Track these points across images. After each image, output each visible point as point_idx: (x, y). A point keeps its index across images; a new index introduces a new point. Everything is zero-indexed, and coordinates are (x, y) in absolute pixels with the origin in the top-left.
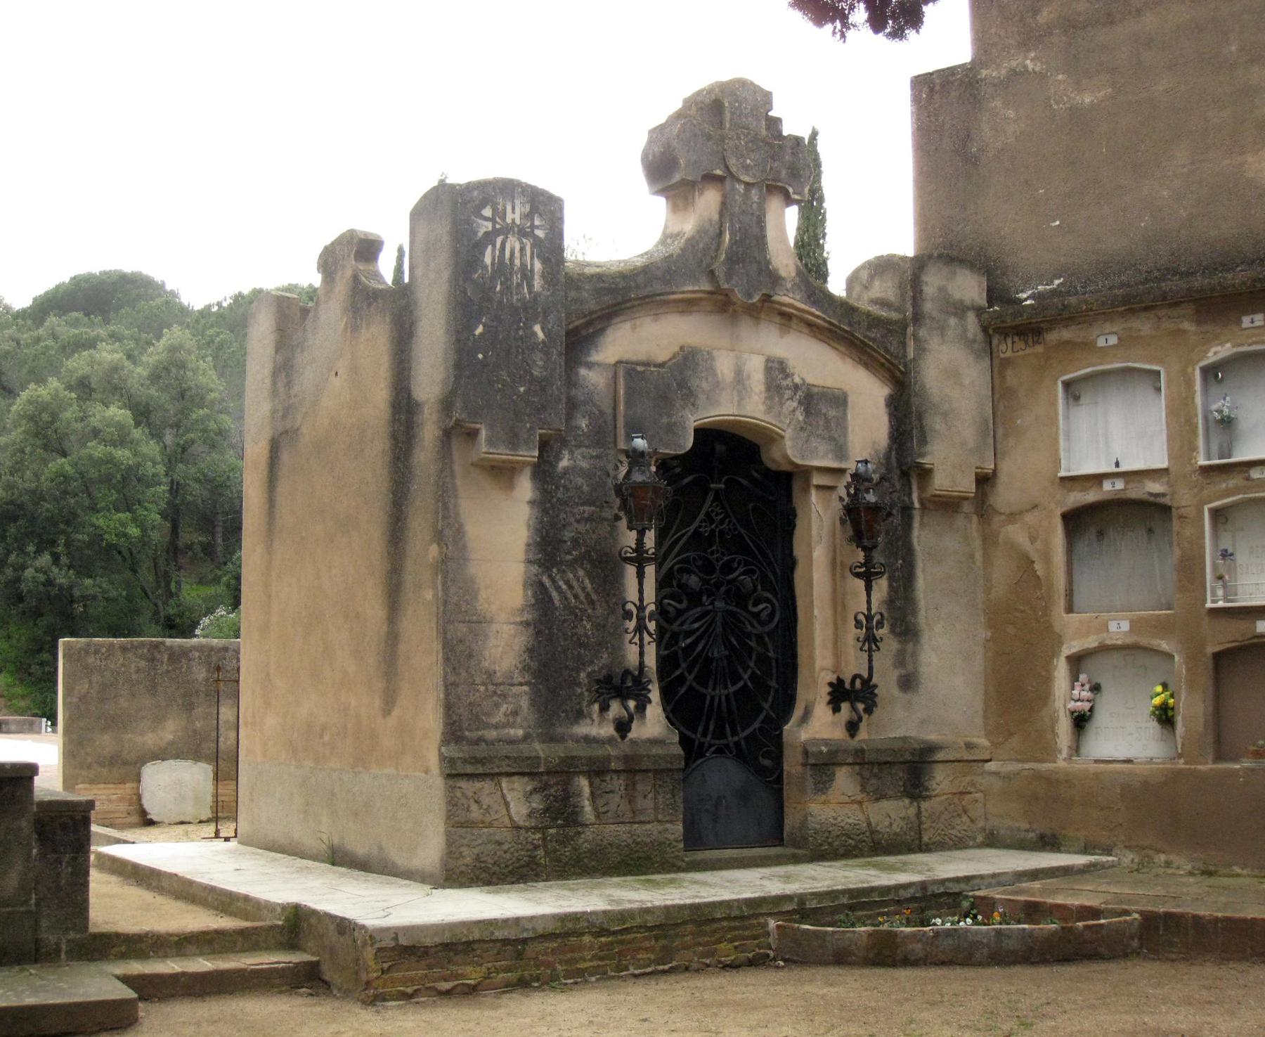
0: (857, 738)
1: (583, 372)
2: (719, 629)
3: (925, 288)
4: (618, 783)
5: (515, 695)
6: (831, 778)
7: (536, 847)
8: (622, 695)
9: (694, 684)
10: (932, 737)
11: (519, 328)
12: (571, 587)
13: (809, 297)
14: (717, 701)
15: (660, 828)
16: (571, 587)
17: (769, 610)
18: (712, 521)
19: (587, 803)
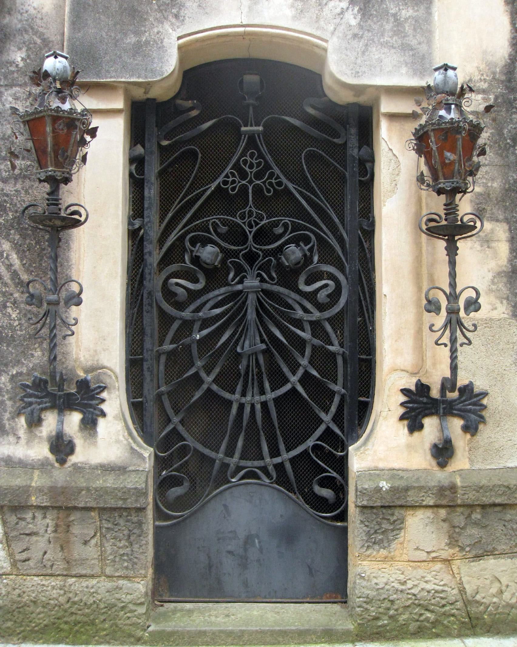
0: (450, 468)
2: (251, 315)
4: (44, 524)
6: (398, 525)
8: (64, 404)
9: (215, 387)
14: (248, 409)
15: (109, 585)
17: (329, 290)
18: (243, 175)
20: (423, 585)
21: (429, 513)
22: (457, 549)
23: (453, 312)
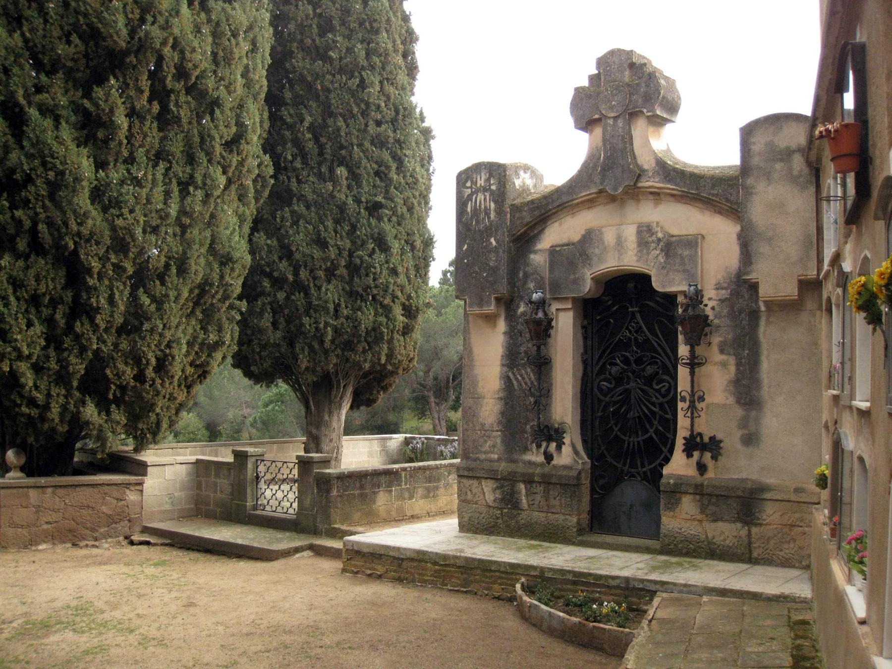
0: (705, 477)
1: (532, 256)
3: (752, 147)
4: (540, 489)
5: (494, 437)
6: (678, 502)
7: (498, 518)
8: (549, 439)
9: (619, 433)
10: (770, 481)
12: (523, 379)
13: (665, 178)
15: (563, 518)
16: (523, 379)
17: (666, 388)
20: (689, 531)
21: (691, 497)
23: (692, 402)
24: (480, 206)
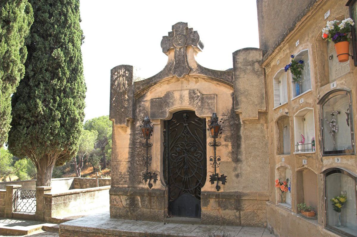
5: (126, 177)
11: (122, 97)
17: (200, 156)
19: (140, 203)
22: (220, 208)
23: (215, 161)
24: (121, 83)
